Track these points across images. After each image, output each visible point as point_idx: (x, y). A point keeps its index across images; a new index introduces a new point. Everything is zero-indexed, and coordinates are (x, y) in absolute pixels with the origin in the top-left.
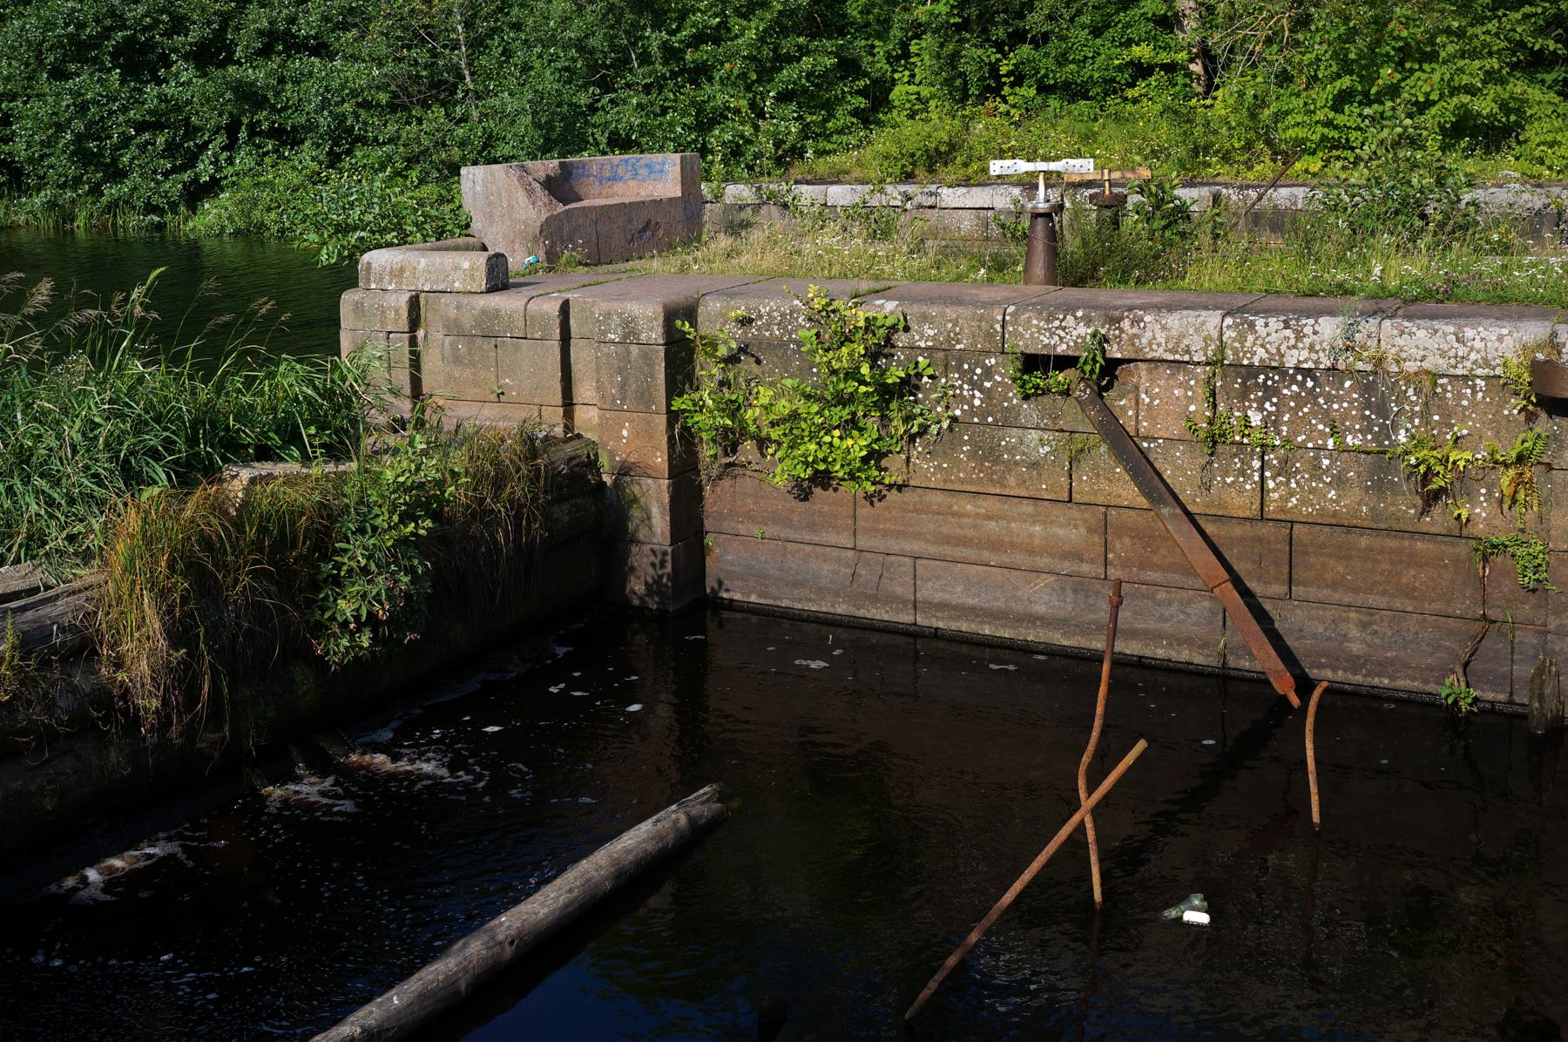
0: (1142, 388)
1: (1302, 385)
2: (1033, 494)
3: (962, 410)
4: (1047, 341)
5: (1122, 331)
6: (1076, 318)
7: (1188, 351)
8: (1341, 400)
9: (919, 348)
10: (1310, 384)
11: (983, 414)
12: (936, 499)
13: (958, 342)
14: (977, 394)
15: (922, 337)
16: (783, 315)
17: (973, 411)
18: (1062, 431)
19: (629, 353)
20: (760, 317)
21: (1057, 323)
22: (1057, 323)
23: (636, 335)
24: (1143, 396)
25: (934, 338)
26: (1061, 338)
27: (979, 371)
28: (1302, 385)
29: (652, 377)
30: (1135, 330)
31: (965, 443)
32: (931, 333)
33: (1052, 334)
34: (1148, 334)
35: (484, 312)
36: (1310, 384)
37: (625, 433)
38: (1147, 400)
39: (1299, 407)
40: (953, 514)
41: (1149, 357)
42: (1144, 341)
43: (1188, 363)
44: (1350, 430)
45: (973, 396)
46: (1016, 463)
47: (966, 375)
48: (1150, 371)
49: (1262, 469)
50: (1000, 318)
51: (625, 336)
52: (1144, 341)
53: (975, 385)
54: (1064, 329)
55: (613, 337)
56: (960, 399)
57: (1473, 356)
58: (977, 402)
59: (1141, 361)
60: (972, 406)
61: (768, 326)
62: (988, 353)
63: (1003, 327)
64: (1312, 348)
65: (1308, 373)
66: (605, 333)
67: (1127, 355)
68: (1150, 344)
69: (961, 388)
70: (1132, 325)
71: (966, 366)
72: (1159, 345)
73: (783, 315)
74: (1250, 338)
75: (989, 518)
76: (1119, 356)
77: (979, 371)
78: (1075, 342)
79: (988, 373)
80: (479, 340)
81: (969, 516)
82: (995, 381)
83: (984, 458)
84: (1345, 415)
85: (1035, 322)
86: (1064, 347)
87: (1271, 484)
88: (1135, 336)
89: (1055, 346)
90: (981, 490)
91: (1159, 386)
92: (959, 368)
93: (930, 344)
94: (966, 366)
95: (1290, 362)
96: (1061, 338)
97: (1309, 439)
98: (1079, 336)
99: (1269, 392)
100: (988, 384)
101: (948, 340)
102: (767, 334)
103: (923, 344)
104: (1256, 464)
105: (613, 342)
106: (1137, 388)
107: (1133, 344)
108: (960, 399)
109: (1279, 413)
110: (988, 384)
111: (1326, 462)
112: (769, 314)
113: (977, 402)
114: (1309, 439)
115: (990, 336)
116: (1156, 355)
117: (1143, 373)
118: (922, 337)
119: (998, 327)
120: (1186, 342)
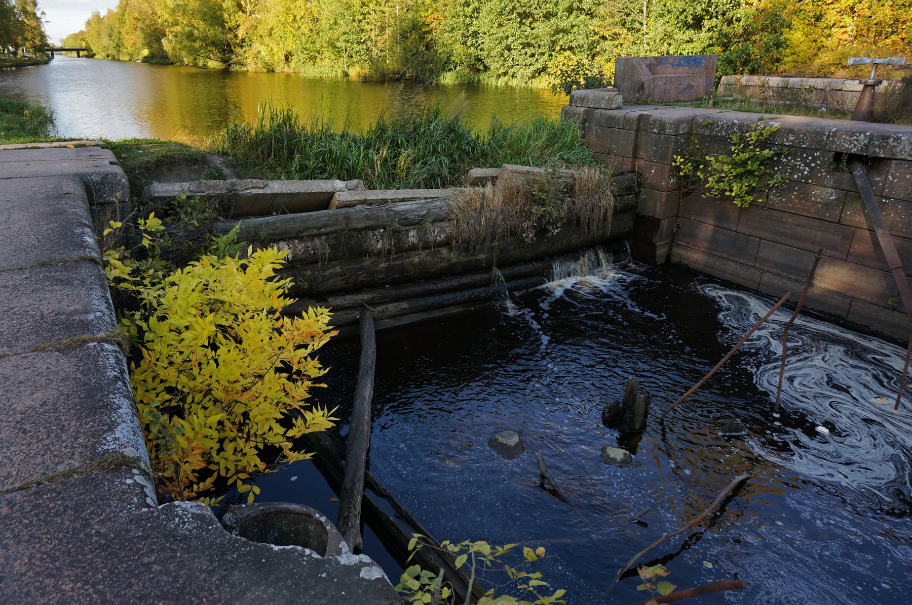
0: (890, 173)
2: (822, 217)
4: (847, 146)
5: (887, 143)
6: (865, 136)
9: (785, 145)
11: (807, 178)
12: (778, 214)
13: (804, 144)
14: (807, 169)
15: (788, 140)
16: (728, 126)
17: (802, 177)
18: (843, 190)
19: (660, 137)
20: (718, 126)
21: (855, 138)
22: (855, 138)
23: (664, 130)
24: (890, 177)
25: (793, 141)
26: (855, 145)
27: (810, 158)
29: (667, 148)
31: (795, 191)
32: (792, 138)
33: (851, 143)
35: (610, 117)
38: (891, 179)
40: (782, 222)
41: (899, 157)
42: (898, 149)
45: (805, 170)
46: (817, 203)
47: (804, 161)
48: (897, 164)
50: (827, 133)
51: (660, 130)
52: (898, 149)
53: (807, 165)
54: (857, 140)
58: (806, 173)
59: (894, 159)
60: (803, 174)
61: (720, 131)
62: (816, 150)
63: (827, 138)
66: (652, 129)
67: (890, 157)
68: (901, 151)
69: (800, 165)
70: (894, 142)
72: (906, 152)
73: (728, 126)
75: (798, 226)
76: (883, 156)
77: (810, 158)
78: (862, 148)
79: (815, 159)
80: (606, 129)
81: (789, 224)
82: (817, 164)
83: (803, 199)
85: (844, 136)
86: (856, 149)
88: (894, 146)
89: (851, 149)
90: (798, 213)
91: (899, 173)
96: (855, 145)
100: (813, 165)
101: (799, 143)
103: (787, 144)
105: (655, 133)
106: (888, 173)
107: (892, 151)
108: (799, 171)
110: (813, 165)
112: (722, 125)
113: (806, 173)
115: (819, 142)
116: (903, 157)
117: (893, 166)
118: (788, 140)
119: (825, 138)
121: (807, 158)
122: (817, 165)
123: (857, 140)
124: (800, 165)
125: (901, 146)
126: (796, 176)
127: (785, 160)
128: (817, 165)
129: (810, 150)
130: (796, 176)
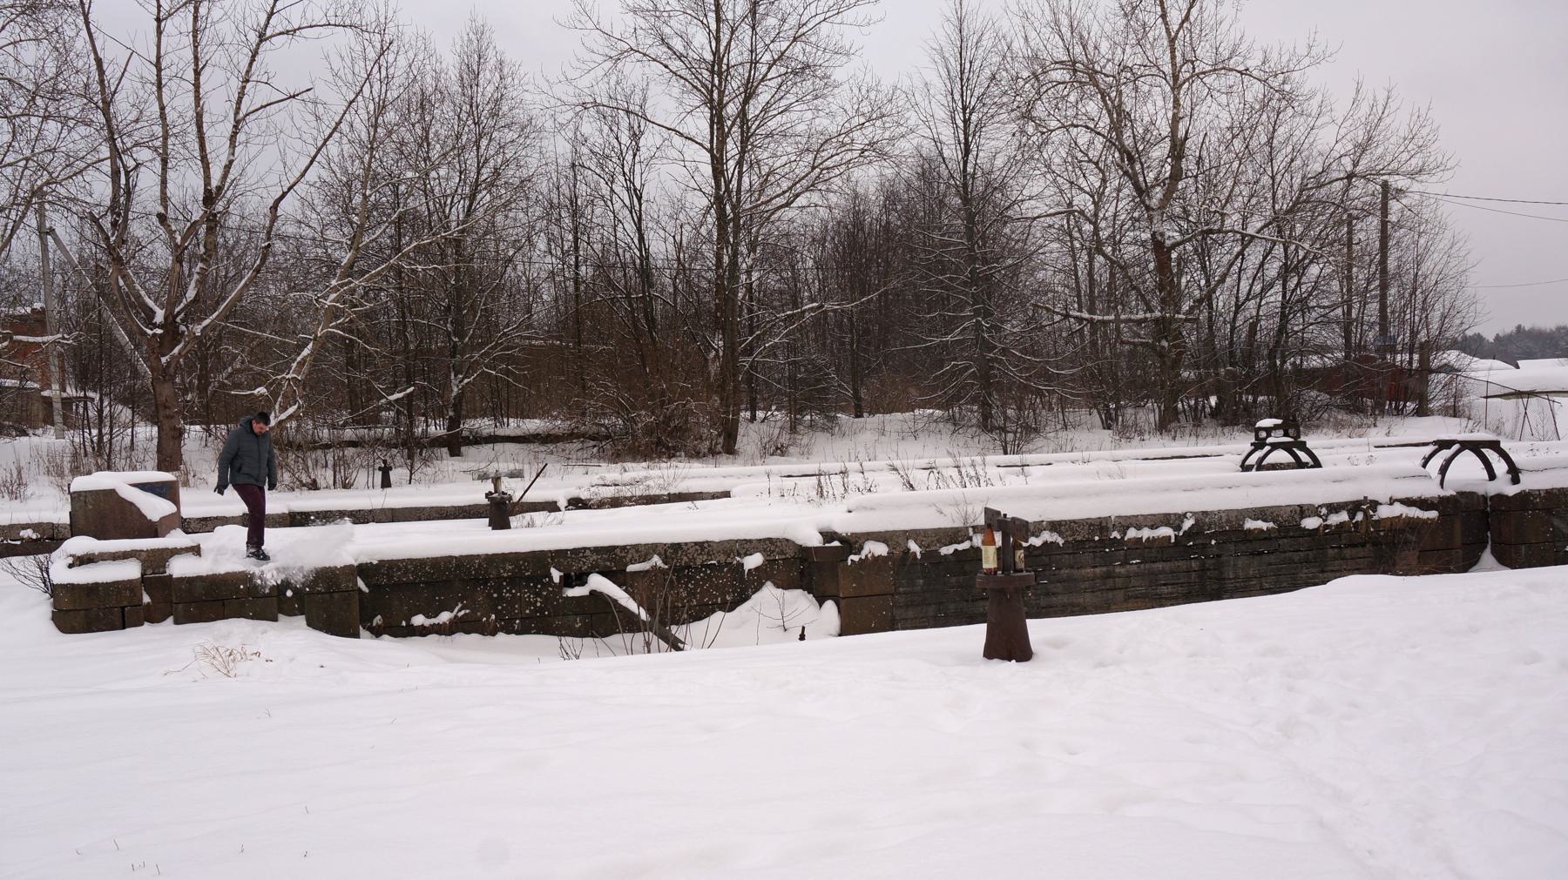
1: (705, 572)
5: (616, 555)
11: (541, 610)
13: (527, 571)
15: (504, 569)
16: (416, 567)
20: (399, 569)
28: (705, 572)
30: (623, 554)
34: (630, 556)
44: (729, 593)
53: (538, 595)
54: (585, 557)
58: (539, 604)
69: (529, 597)
84: (725, 585)
92: (527, 586)
95: (699, 562)
97: (709, 600)
99: (690, 578)
103: (505, 575)
108: (530, 604)
114: (709, 600)
121: (535, 587)
123: (585, 557)
124: (529, 597)
125: (630, 556)
126: (528, 612)
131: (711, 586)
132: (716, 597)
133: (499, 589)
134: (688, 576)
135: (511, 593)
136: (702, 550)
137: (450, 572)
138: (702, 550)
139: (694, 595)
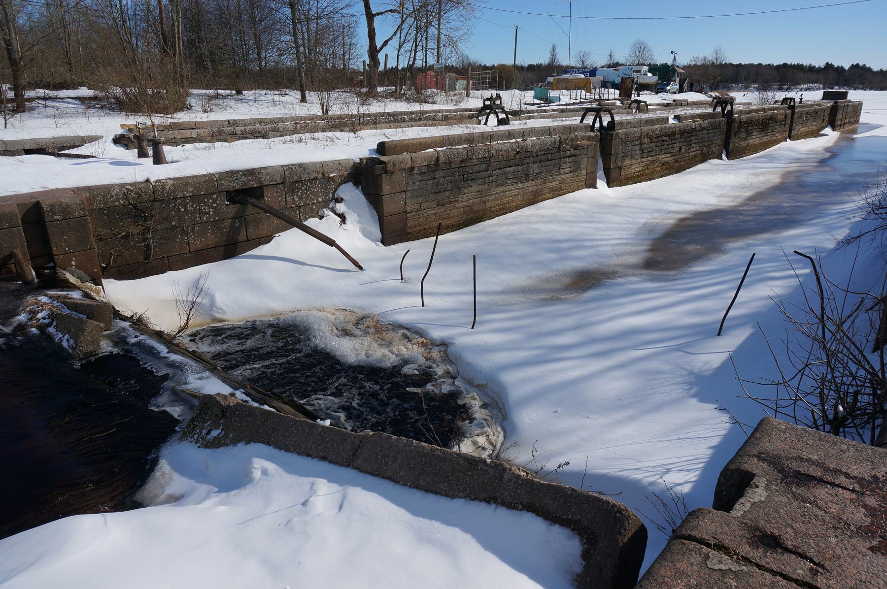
1: (307, 185)
3: (206, 217)
5: (256, 177)
7: (276, 181)
8: (316, 188)
10: (309, 184)
14: (211, 210)
20: (112, 196)
25: (192, 192)
28: (307, 185)
31: (209, 229)
33: (234, 182)
36: (309, 184)
37: (73, 263)
39: (307, 192)
43: (277, 184)
45: (210, 211)
49: (299, 214)
55: (58, 217)
56: (207, 213)
57: (343, 169)
58: (211, 213)
61: (117, 200)
62: (213, 193)
64: (308, 174)
65: (307, 181)
66: (52, 216)
69: (205, 209)
71: (206, 200)
74: (292, 173)
76: (256, 186)
77: (211, 201)
84: (318, 192)
87: (302, 218)
93: (191, 194)
94: (206, 200)
97: (310, 201)
98: (243, 181)
99: (300, 189)
100: (215, 205)
102: (117, 203)
103: (188, 195)
104: (298, 213)
108: (207, 213)
109: (302, 195)
110: (215, 205)
111: (314, 207)
120: (275, 177)
122: (218, 205)
126: (205, 219)
127: (191, 208)
128: (218, 205)
129: (208, 195)
130: (205, 219)
131: (310, 193)
132: (313, 199)
133: (185, 205)
134: (297, 188)
135: (192, 206)
136: (305, 171)
137: (149, 195)
138: (305, 171)
139: (302, 199)
